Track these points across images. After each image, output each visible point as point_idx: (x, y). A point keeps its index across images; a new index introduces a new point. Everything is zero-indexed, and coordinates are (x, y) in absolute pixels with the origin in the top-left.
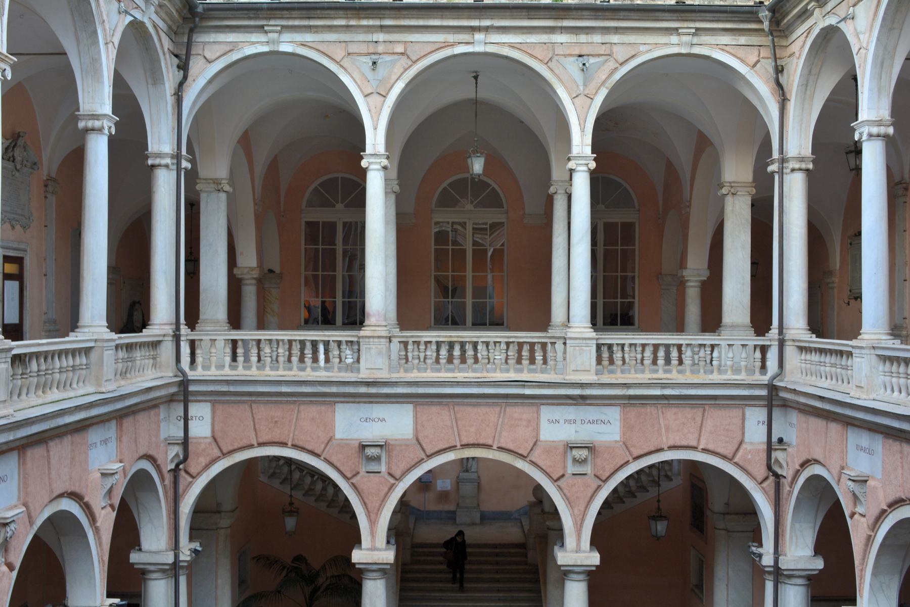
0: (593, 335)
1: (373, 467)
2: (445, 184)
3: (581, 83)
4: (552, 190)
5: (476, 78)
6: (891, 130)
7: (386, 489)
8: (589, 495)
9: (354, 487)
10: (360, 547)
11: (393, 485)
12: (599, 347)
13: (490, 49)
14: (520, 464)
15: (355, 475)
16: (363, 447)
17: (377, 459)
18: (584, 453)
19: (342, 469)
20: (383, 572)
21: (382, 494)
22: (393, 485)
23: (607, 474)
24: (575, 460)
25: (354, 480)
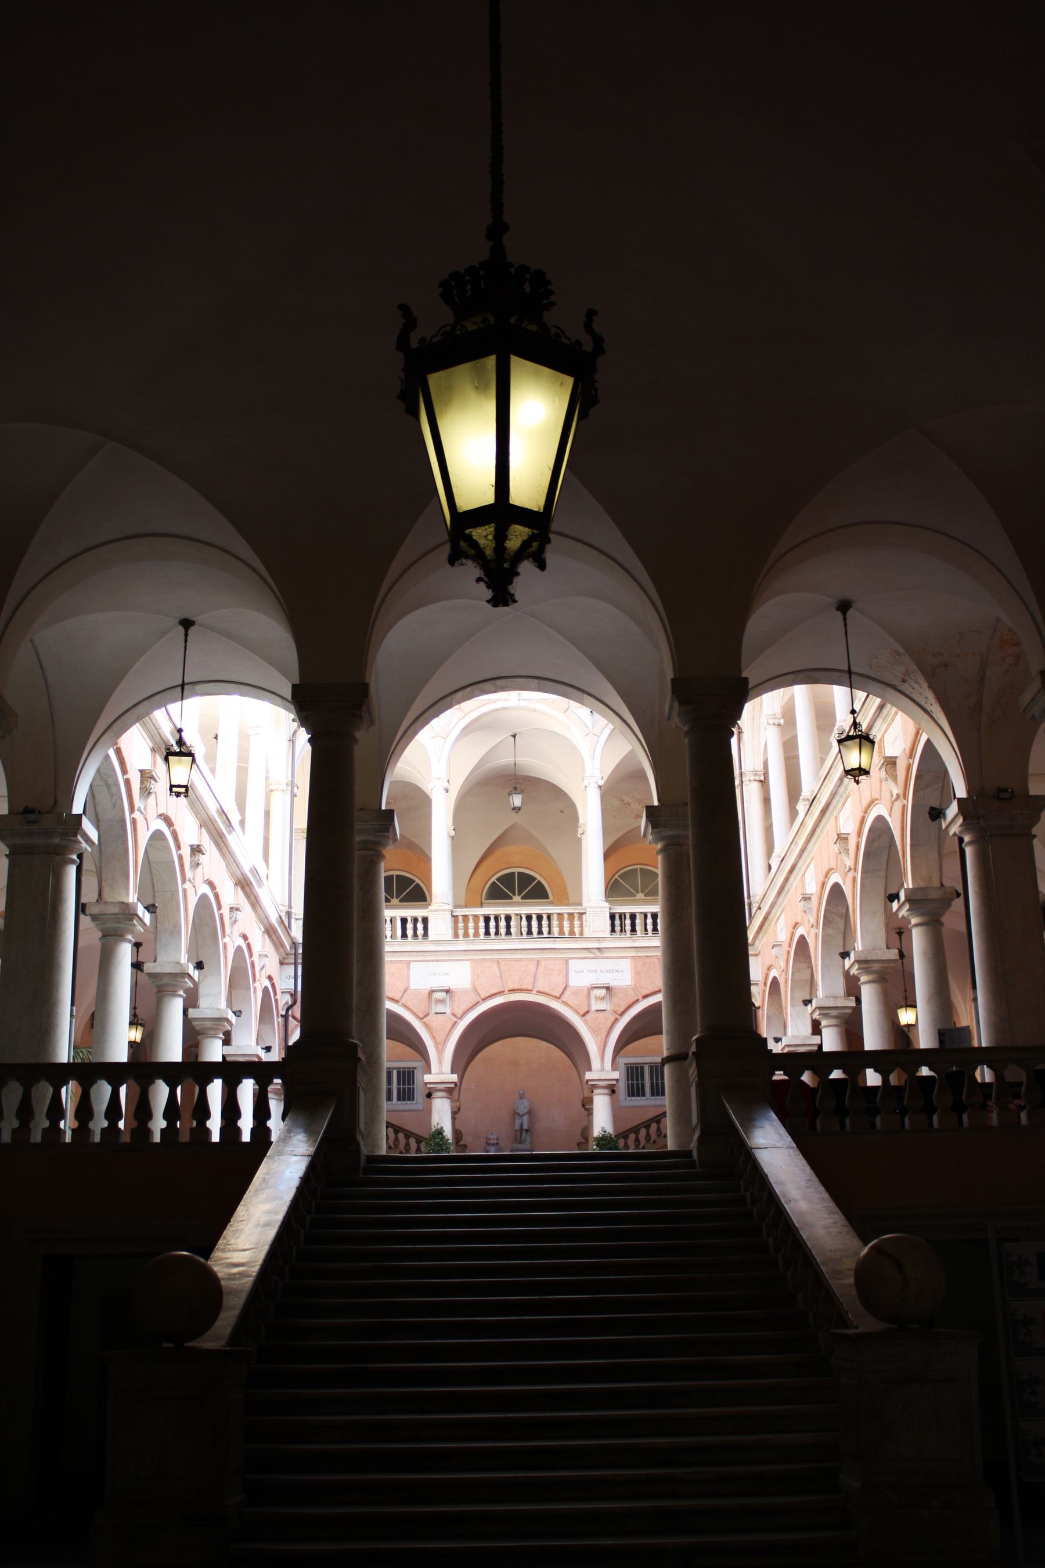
0: (607, 904)
1: (440, 1008)
2: (494, 879)
3: (589, 724)
4: (580, 831)
5: (514, 736)
6: (782, 721)
7: (450, 1026)
8: (609, 1026)
9: (426, 1025)
10: (429, 1071)
11: (456, 1022)
12: (612, 917)
13: (523, 704)
14: (555, 1005)
15: (425, 1016)
16: (433, 991)
17: (441, 1001)
18: (603, 992)
19: (416, 1011)
20: (449, 1091)
21: (448, 1029)
22: (456, 1022)
23: (622, 1009)
24: (597, 998)
25: (425, 1020)
